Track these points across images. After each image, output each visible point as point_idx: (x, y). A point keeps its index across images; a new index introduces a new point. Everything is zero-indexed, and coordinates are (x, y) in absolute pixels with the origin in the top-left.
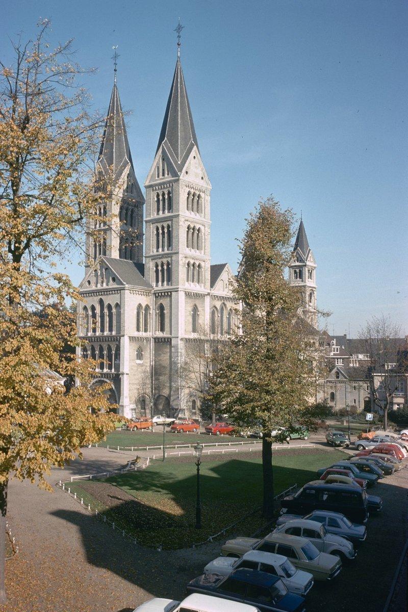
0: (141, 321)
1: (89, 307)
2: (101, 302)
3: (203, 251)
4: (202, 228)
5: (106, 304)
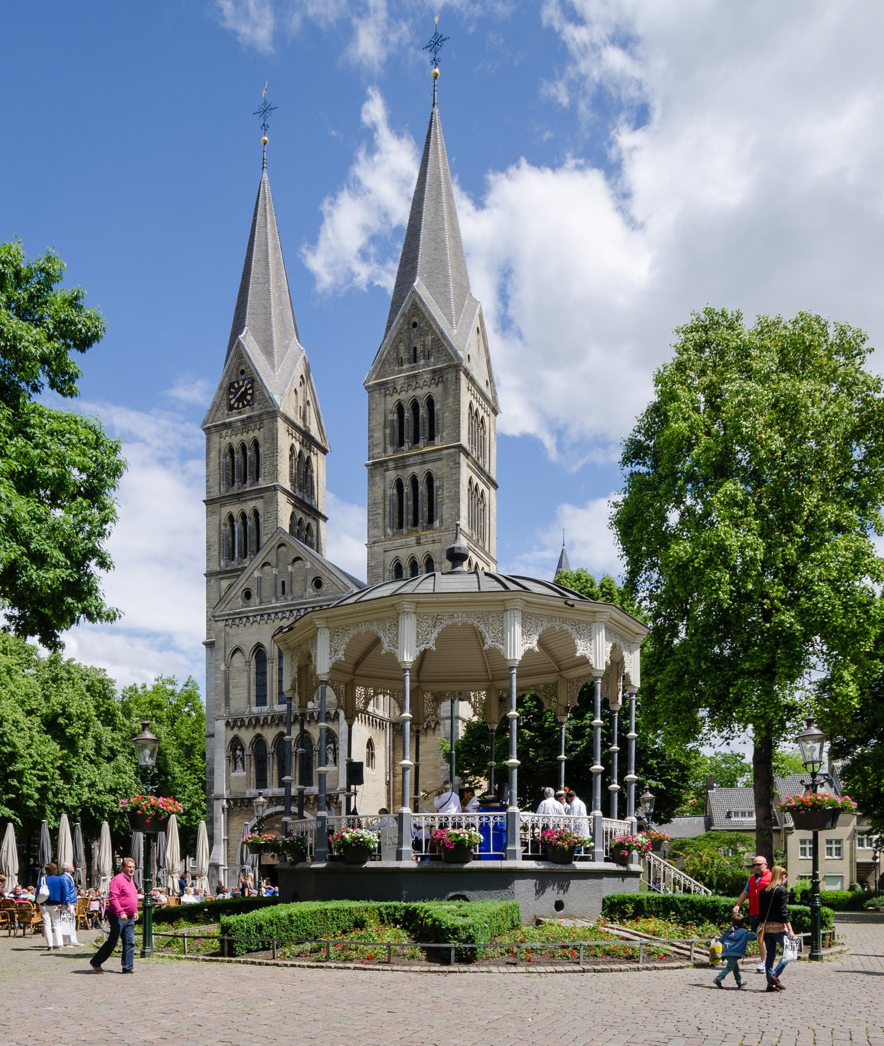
1: (248, 649)
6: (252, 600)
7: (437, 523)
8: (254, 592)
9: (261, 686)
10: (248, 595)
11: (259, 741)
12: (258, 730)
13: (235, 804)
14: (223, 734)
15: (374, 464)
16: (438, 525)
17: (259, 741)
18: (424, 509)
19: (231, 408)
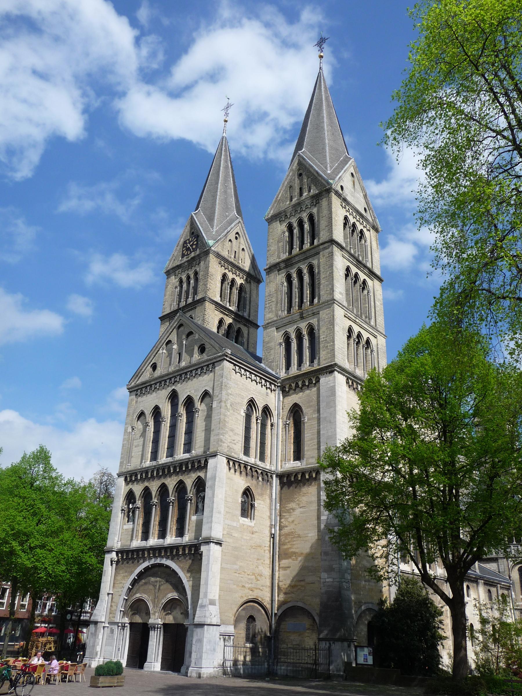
0: (255, 435)
2: (174, 397)
5: (182, 398)
6: (156, 371)
7: (316, 301)
8: (158, 365)
9: (156, 441)
10: (154, 367)
11: (147, 493)
12: (146, 484)
13: (122, 557)
14: (120, 489)
15: (270, 268)
16: (316, 302)
17: (147, 493)
18: (307, 292)
19: (183, 256)
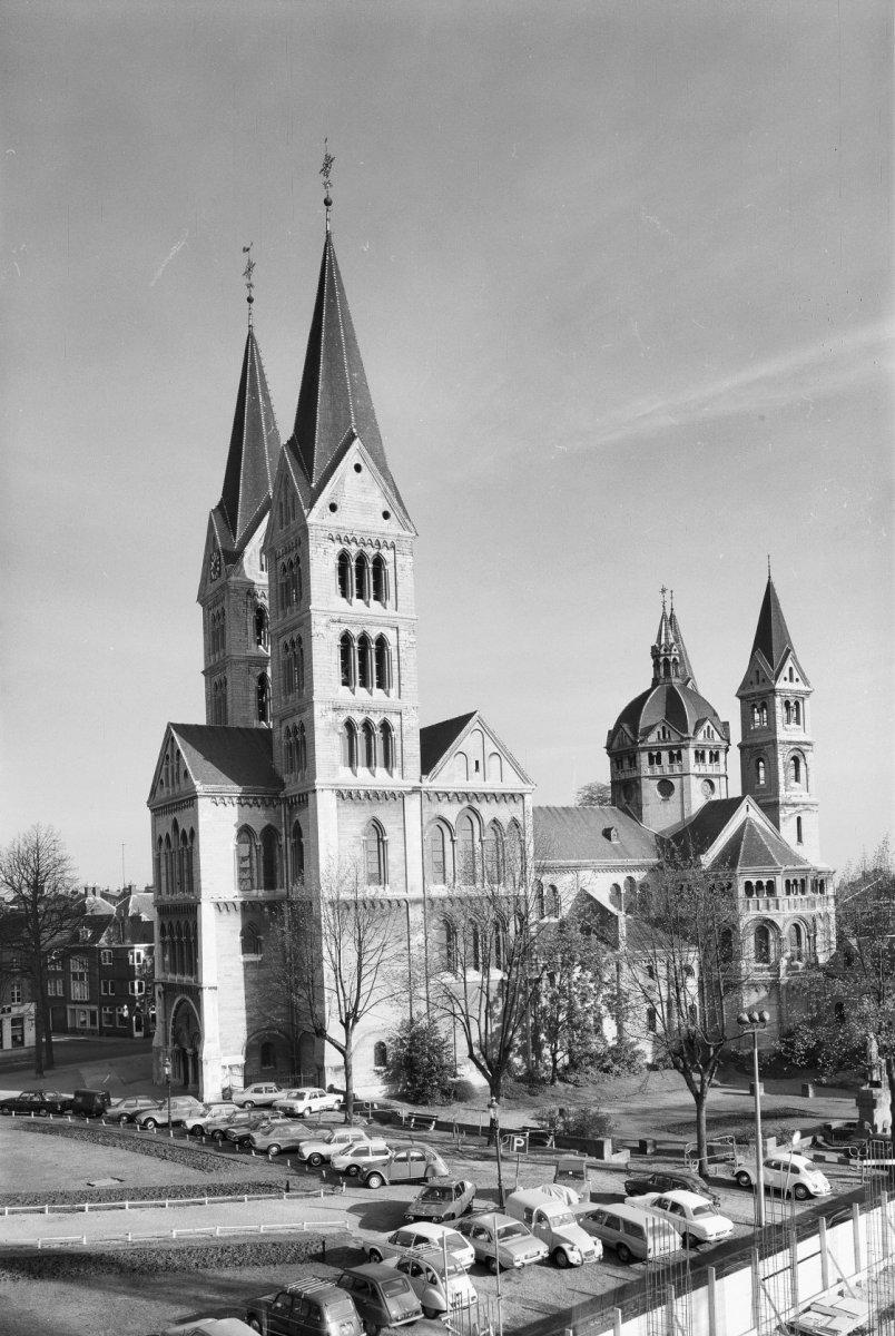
2: (175, 825)
3: (393, 691)
4: (390, 636)
